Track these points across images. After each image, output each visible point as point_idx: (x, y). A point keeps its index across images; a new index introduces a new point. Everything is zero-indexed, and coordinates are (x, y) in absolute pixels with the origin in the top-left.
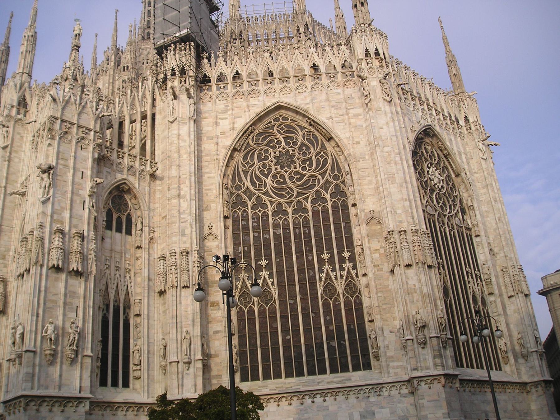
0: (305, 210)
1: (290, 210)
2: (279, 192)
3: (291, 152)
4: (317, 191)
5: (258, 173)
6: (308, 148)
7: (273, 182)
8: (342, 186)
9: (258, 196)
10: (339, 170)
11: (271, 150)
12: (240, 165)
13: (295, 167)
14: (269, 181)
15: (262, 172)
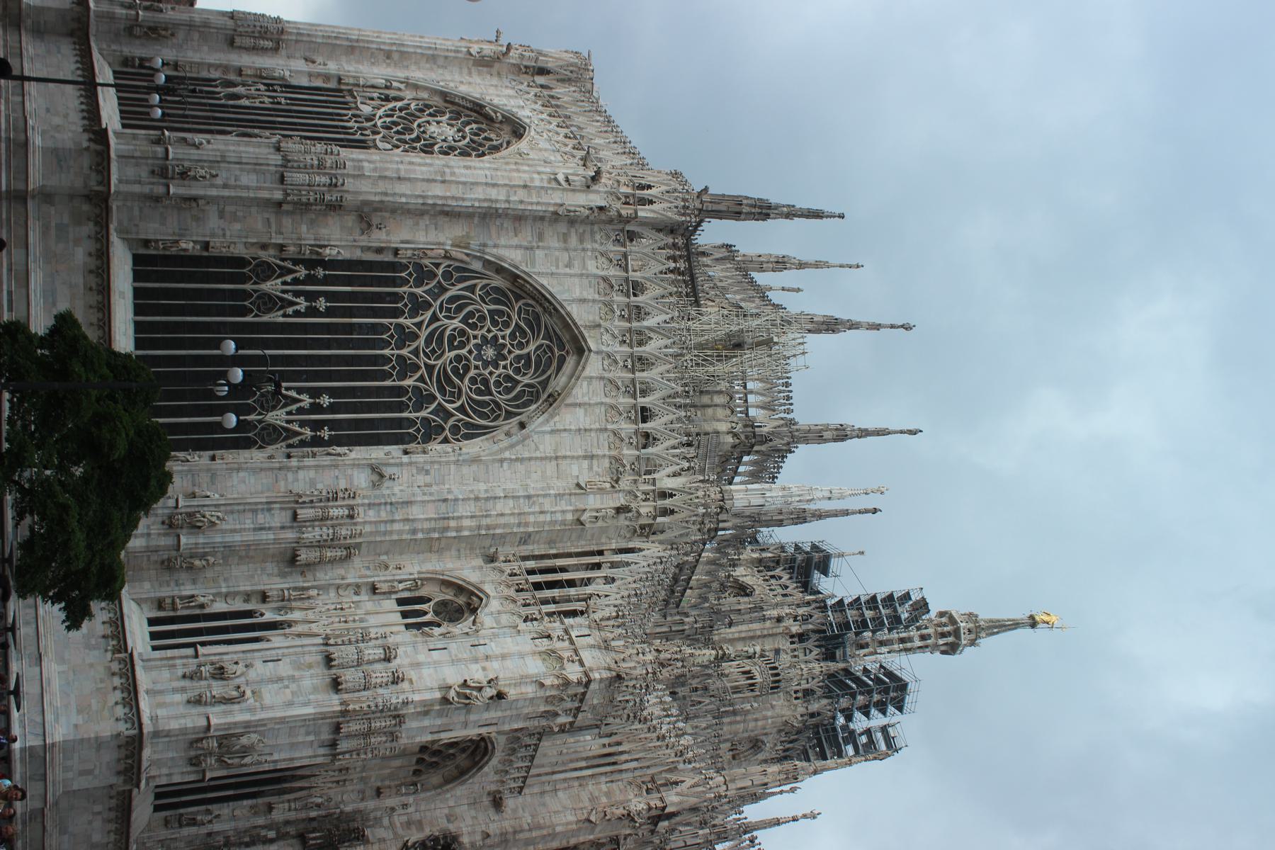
0: (402, 377)
1: (405, 352)
2: (436, 338)
3: (502, 363)
4: (435, 398)
5: (470, 308)
6: (508, 390)
7: (454, 330)
8: (441, 438)
9: (431, 305)
10: (468, 437)
11: (508, 332)
12: (485, 282)
13: (477, 367)
14: (456, 323)
15: (471, 315)
